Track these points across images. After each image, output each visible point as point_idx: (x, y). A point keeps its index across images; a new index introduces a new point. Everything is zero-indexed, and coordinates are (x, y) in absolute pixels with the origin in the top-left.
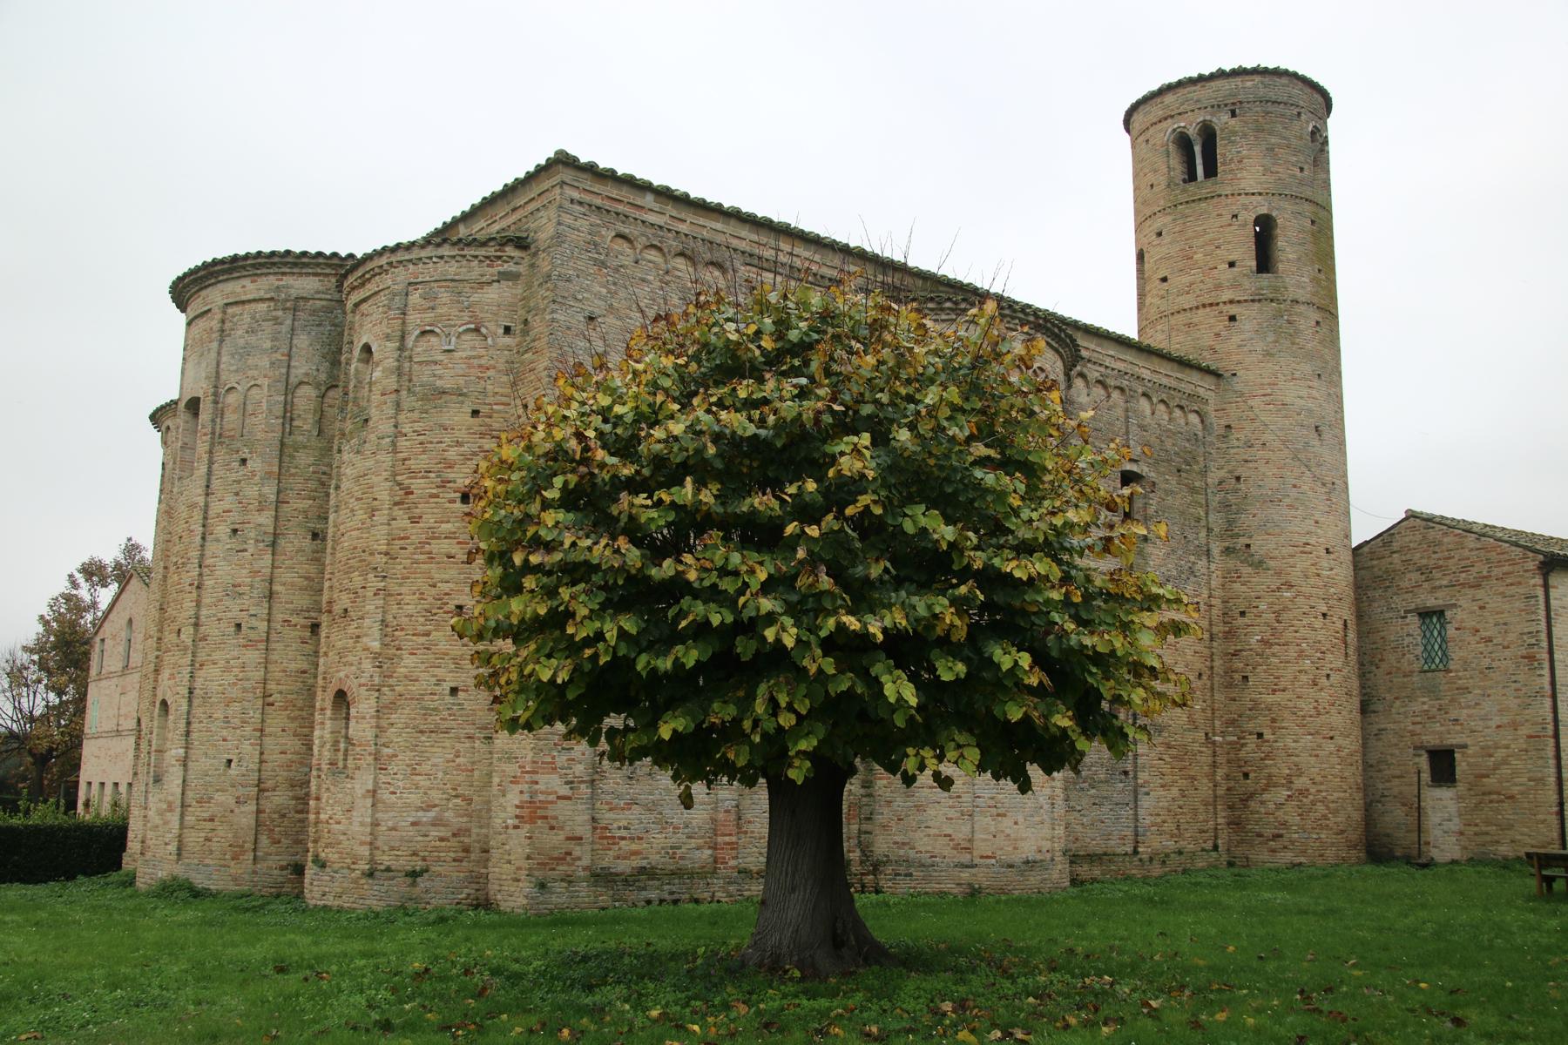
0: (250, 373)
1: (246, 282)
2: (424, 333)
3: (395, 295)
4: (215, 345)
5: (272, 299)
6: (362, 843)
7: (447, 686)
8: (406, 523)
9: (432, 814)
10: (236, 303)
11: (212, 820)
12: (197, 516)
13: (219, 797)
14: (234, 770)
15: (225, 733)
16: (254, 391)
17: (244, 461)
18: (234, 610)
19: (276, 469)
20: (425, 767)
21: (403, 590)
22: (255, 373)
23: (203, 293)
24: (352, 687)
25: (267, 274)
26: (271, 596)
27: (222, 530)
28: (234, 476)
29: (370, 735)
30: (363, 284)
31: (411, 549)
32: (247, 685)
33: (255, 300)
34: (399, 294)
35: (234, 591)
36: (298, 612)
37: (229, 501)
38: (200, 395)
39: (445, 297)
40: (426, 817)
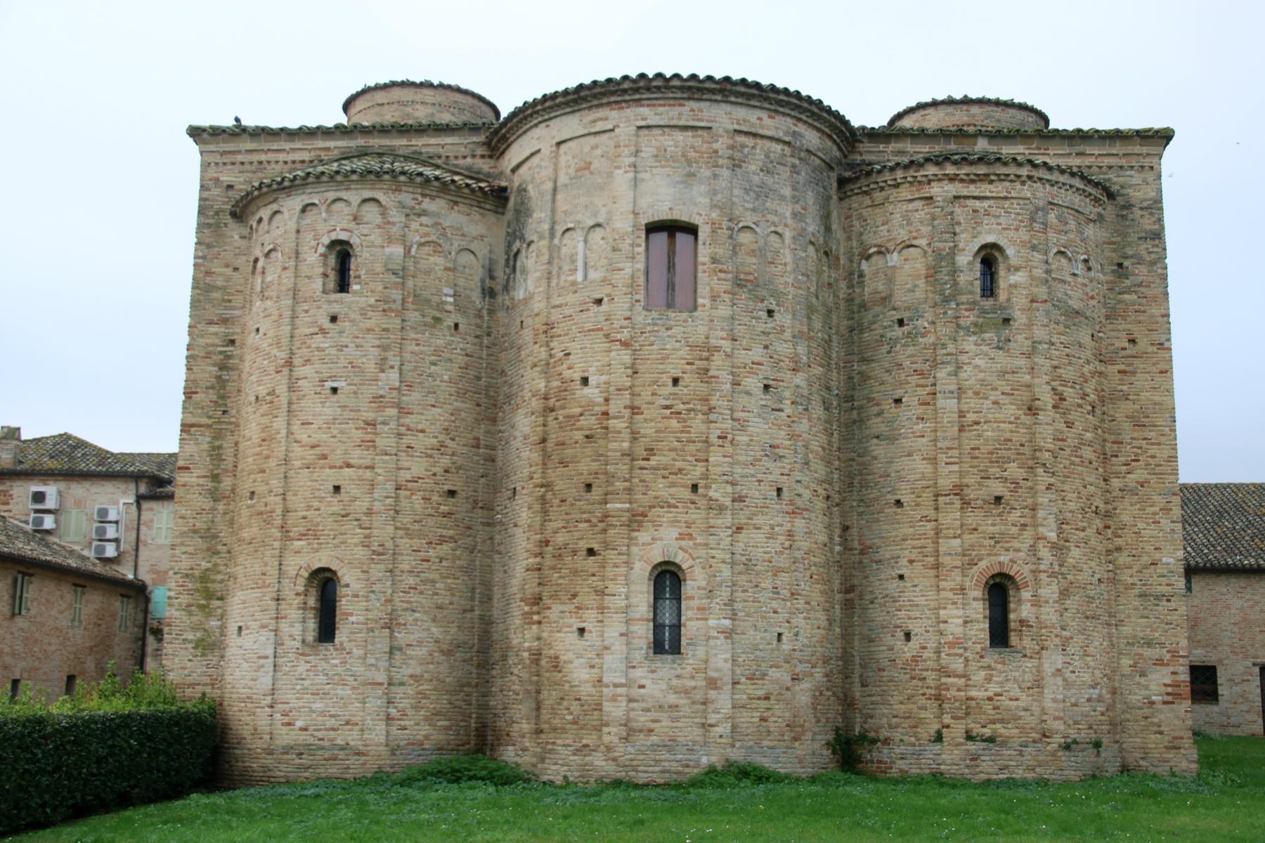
0: (770, 217)
1: (764, 115)
2: (1060, 252)
3: (1038, 209)
4: (725, 173)
5: (788, 143)
6: (1057, 718)
8: (1062, 426)
9: (1097, 691)
10: (747, 134)
11: (767, 698)
13: (774, 673)
14: (786, 646)
15: (775, 604)
16: (774, 238)
17: (770, 313)
18: (775, 471)
19: (805, 329)
20: (1090, 650)
21: (1066, 487)
22: (776, 219)
23: (692, 104)
24: (1021, 570)
25: (784, 114)
27: (753, 383)
28: (761, 327)
29: (1054, 618)
30: (972, 181)
31: (1068, 451)
32: (798, 554)
33: (771, 138)
34: (1043, 209)
37: (757, 353)
39: (1072, 225)
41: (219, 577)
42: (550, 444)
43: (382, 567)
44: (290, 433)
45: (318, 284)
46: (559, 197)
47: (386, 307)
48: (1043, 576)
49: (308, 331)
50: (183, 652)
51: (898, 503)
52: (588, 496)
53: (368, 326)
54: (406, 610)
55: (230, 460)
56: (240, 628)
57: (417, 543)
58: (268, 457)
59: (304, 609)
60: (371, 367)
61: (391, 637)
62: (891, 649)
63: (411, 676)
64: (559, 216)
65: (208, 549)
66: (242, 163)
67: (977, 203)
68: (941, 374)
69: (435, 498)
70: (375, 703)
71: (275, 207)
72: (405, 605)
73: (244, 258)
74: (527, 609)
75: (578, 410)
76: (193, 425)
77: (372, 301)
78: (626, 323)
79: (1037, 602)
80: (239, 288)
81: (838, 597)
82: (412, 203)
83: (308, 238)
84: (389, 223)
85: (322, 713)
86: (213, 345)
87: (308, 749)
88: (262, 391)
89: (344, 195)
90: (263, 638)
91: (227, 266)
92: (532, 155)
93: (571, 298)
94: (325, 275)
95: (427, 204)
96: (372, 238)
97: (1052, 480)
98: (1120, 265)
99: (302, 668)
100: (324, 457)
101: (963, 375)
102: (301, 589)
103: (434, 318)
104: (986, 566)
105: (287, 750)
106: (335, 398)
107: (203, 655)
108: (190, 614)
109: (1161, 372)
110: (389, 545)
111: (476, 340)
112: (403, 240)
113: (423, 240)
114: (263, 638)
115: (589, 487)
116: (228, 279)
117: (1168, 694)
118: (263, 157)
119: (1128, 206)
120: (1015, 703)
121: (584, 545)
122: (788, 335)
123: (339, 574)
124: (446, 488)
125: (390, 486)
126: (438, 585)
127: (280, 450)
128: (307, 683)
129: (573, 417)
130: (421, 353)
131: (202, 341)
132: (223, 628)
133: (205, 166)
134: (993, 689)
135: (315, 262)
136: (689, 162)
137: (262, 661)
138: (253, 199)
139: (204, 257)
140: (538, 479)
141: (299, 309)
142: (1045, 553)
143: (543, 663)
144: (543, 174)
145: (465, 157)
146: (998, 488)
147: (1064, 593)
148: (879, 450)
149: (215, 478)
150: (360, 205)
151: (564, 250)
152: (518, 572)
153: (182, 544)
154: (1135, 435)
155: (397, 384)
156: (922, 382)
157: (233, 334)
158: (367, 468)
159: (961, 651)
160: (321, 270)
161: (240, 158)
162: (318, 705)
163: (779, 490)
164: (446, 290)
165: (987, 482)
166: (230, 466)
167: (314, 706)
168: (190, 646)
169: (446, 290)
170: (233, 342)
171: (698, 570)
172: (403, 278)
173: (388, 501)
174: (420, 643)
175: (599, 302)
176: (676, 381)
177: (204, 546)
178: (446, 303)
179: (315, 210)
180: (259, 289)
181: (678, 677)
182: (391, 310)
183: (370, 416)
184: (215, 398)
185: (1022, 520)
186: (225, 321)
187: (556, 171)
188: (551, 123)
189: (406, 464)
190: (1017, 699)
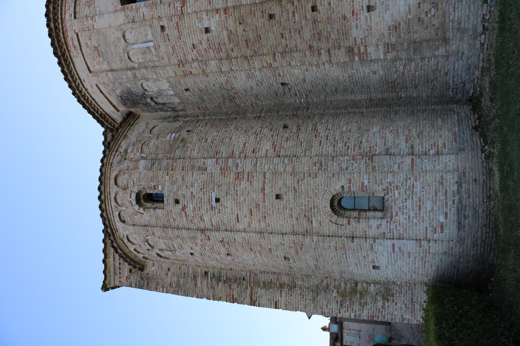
41: (343, 284)
42: (248, 53)
43: (330, 163)
44: (245, 231)
45: (159, 212)
46: (114, 67)
47: (170, 168)
49: (185, 218)
50: (391, 309)
52: (277, 16)
53: (181, 180)
54: (360, 148)
55: (271, 276)
56: (374, 267)
57: (315, 144)
58: (261, 246)
59: (359, 218)
60: (204, 177)
61: (379, 155)
63: (406, 142)
64: (123, 66)
65: (325, 291)
66: (120, 264)
69: (286, 135)
70: (427, 164)
71: (125, 240)
72: (357, 148)
73: (163, 264)
74: (357, 59)
75: (225, 33)
76: (251, 298)
77: (167, 177)
78: (172, 5)
80: (178, 269)
82: (120, 156)
84: (127, 169)
85: (434, 202)
86: (207, 285)
87: (460, 211)
88: (223, 251)
89: (113, 196)
90: (380, 248)
91: (167, 274)
92: (101, 92)
93: (163, 49)
94: (154, 209)
95: (121, 150)
96: (135, 179)
99: (401, 218)
100: (257, 206)
102: (345, 221)
103: (181, 142)
105: (460, 226)
106: (222, 200)
107: (393, 295)
108: (366, 304)
110: (315, 159)
111: (200, 122)
112: (137, 161)
113: (140, 151)
114: (380, 248)
115: (271, 16)
116: (173, 274)
121: (309, 14)
123: (335, 193)
124: (281, 129)
125: (276, 160)
127: (254, 237)
128: (412, 214)
129: (229, 36)
130: (199, 147)
131: (205, 291)
132: (376, 283)
135: (149, 215)
137: (396, 249)
138: (125, 254)
139: (163, 287)
140: (269, 59)
141: (173, 225)
143: (394, 40)
144: (106, 80)
149: (282, 286)
150: (118, 187)
151: (141, 60)
152: (332, 71)
153: (322, 308)
155: (214, 159)
157: (201, 273)
158: (265, 177)
160: (152, 210)
161: (117, 265)
162: (429, 205)
164: (168, 138)
166: (275, 276)
167: (429, 208)
168: (386, 304)
169: (168, 138)
170: (206, 273)
172: (156, 160)
173: (286, 162)
175: (163, 28)
177: (323, 293)
178: (175, 137)
179: (122, 214)
180: (170, 253)
182: (172, 166)
183: (232, 176)
184: (236, 285)
186: (195, 277)
187: (102, 72)
188: (82, 78)
189: (264, 152)
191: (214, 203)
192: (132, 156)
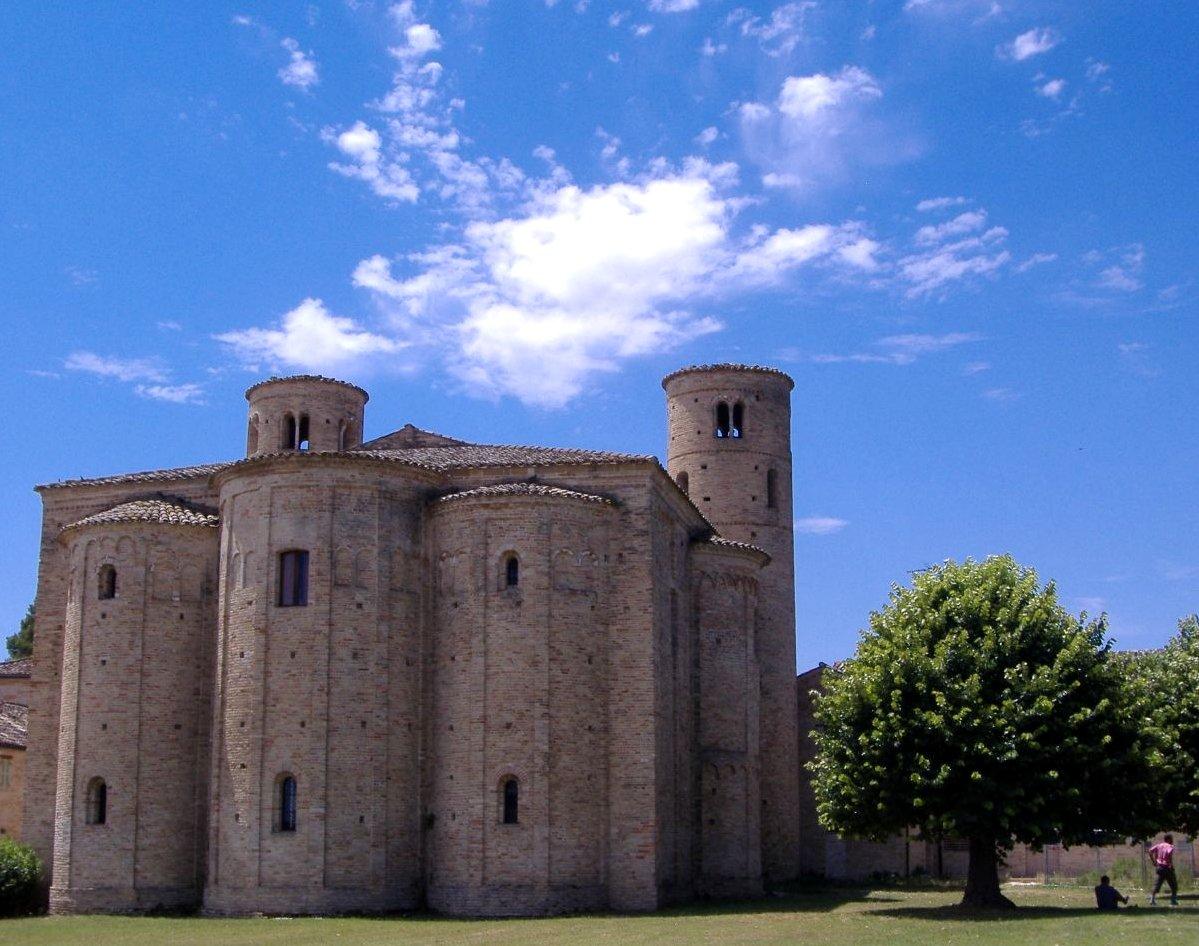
4: (327, 515)
7: (586, 775)
8: (559, 673)
12: (321, 643)
24: (521, 771)
26: (388, 704)
27: (343, 652)
29: (545, 802)
35: (360, 696)
36: (402, 715)
38: (308, 547)
40: (579, 852)
48: (536, 775)
51: (451, 728)
57: (153, 760)
60: (125, 645)
61: (137, 820)
62: (445, 825)
65: (47, 764)
67: (502, 523)
68: (475, 641)
72: (147, 800)
77: (126, 603)
79: (532, 793)
81: (420, 790)
83: (91, 562)
86: (50, 629)
97: (547, 711)
98: (621, 555)
99: (86, 840)
101: (490, 641)
102: (85, 790)
104: (500, 770)
109: (645, 629)
117: (640, 851)
118: (79, 504)
119: (628, 512)
120: (515, 860)
122: (373, 618)
126: (168, 787)
128: (89, 849)
133: (46, 511)
134: (501, 850)
136: (304, 509)
139: (44, 571)
142: (539, 761)
145: (201, 497)
146: (509, 718)
147: (552, 787)
148: (443, 692)
150: (119, 541)
154: (626, 674)
155: (140, 657)
156: (465, 646)
159: (481, 827)
162: (95, 864)
163: (364, 724)
165: (504, 714)
171: (304, 776)
174: (156, 824)
176: (293, 655)
181: (291, 845)
183: (124, 678)
185: (525, 738)
190: (516, 857)
191: (101, 659)
192: (153, 552)
